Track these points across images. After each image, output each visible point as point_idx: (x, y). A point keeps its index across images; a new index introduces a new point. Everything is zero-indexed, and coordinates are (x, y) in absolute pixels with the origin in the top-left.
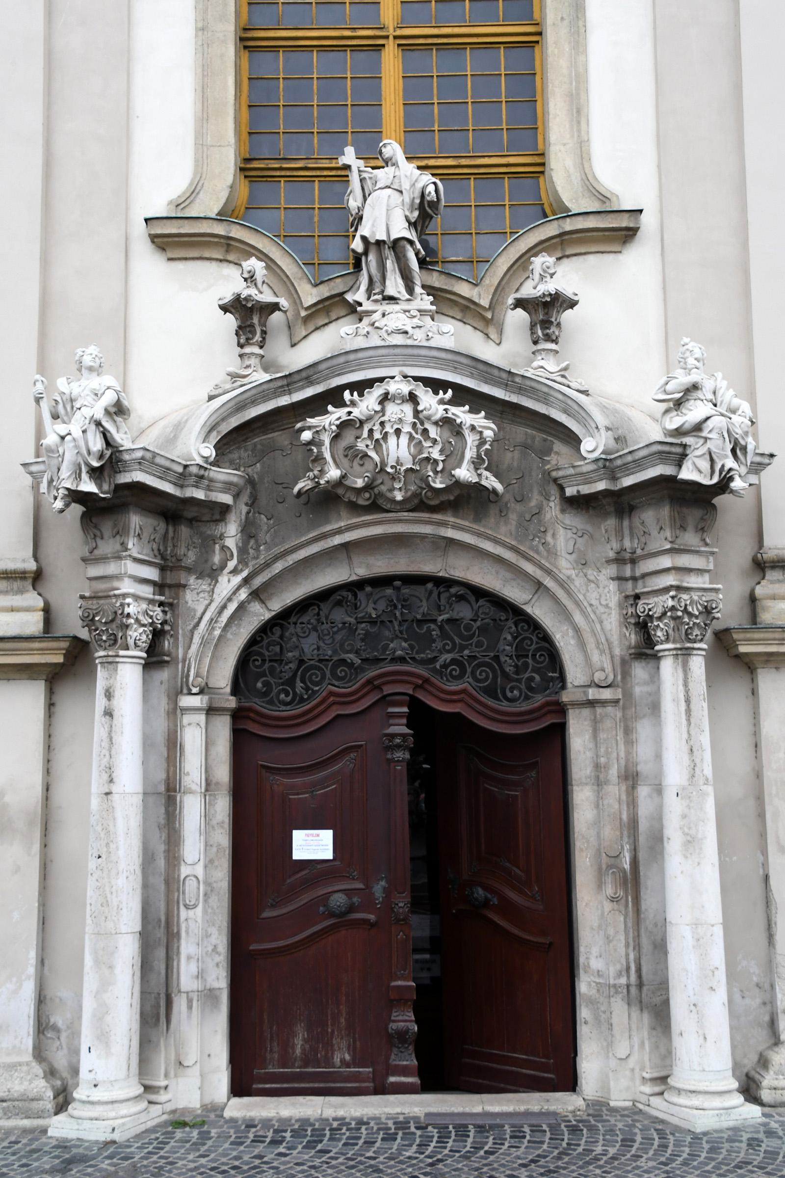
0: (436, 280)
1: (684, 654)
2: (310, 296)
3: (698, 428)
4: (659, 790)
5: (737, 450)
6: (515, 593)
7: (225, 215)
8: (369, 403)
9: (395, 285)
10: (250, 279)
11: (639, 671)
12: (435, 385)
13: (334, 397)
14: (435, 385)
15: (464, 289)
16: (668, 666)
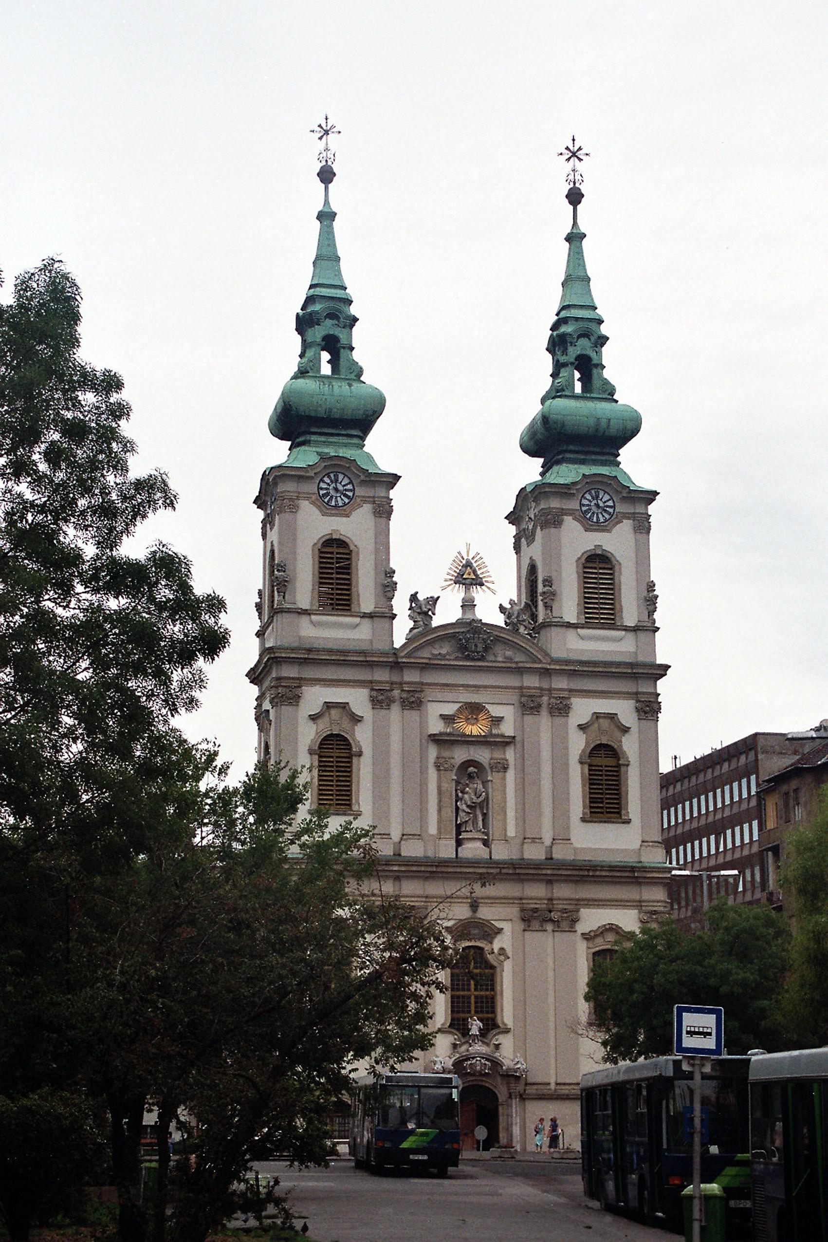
0: (481, 1038)
1: (516, 1098)
2: (463, 1041)
3: (519, 1068)
4: (512, 1116)
5: (524, 1071)
6: (491, 1087)
7: (450, 1026)
8: (474, 1061)
9: (476, 1041)
10: (455, 1039)
11: (510, 1100)
12: (483, 1058)
13: (468, 1059)
14: (483, 1058)
15: (486, 1041)
16: (514, 1101)
